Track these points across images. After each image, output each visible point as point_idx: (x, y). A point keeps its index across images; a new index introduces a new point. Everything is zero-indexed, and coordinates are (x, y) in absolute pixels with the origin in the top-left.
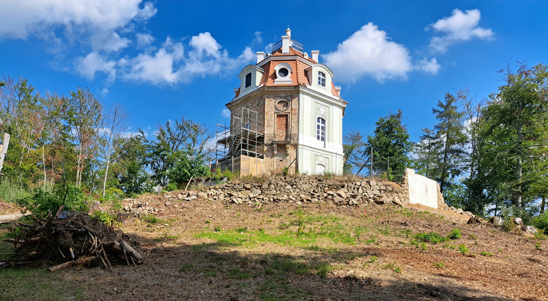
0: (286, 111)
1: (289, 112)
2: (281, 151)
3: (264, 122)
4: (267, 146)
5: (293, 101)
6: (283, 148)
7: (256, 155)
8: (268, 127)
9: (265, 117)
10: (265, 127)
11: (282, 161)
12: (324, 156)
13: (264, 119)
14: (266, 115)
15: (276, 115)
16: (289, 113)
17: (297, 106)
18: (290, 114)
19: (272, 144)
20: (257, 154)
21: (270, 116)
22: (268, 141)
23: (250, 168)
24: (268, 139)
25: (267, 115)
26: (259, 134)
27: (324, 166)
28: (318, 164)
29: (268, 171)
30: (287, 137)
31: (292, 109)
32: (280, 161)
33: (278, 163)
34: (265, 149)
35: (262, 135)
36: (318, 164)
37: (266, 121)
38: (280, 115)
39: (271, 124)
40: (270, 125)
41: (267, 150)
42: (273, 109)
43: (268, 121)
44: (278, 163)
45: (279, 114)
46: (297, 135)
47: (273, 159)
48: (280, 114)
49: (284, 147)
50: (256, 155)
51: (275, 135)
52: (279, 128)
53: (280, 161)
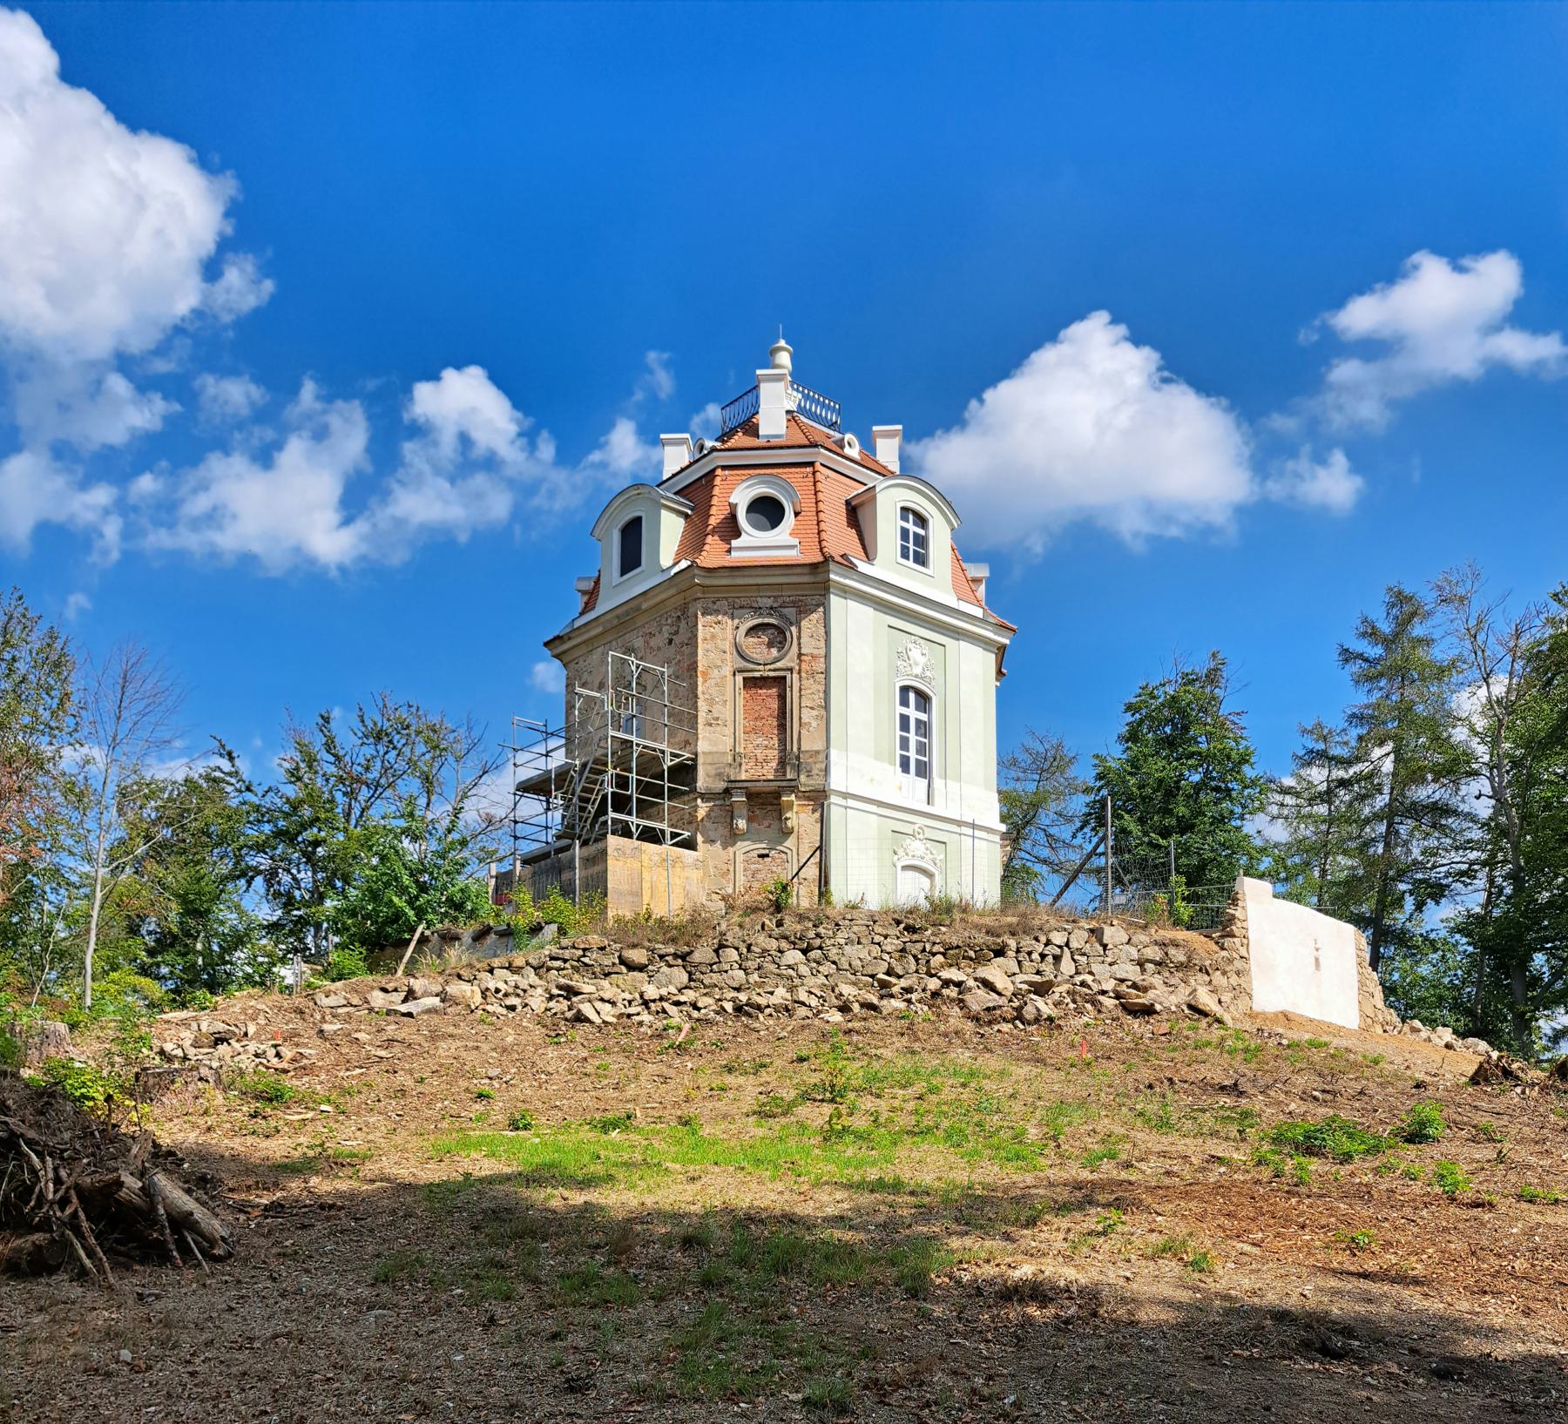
4: (708, 800)
6: (770, 808)
7: (668, 836)
8: (711, 725)
9: (700, 689)
10: (700, 727)
11: (767, 856)
12: (929, 834)
13: (696, 696)
19: (727, 791)
20: (668, 830)
25: (705, 681)
27: (930, 875)
28: (905, 868)
35: (688, 759)
36: (905, 868)
37: (700, 703)
40: (717, 719)
41: (708, 815)
43: (711, 702)
49: (775, 802)
50: (668, 836)
51: (738, 759)
52: (754, 730)
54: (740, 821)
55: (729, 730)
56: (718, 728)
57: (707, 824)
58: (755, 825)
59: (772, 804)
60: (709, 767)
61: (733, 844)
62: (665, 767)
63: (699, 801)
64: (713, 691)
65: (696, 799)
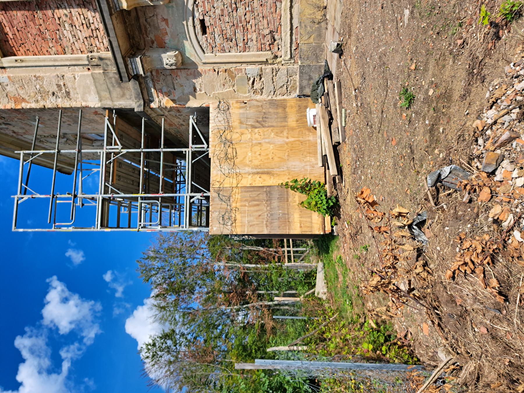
2: (157, 28)
3: (56, 109)
4: (150, 95)
6: (142, 20)
8: (68, 93)
9: (34, 105)
10: (74, 104)
11: (202, 22)
13: (43, 110)
19: (137, 77)
20: (192, 148)
21: (22, 87)
23: (259, 181)
24: (118, 90)
25: (24, 100)
26: (109, 133)
29: (256, 86)
32: (204, 32)
33: (218, 41)
34: (166, 102)
35: (110, 120)
37: (49, 105)
39: (54, 82)
40: (59, 86)
41: (168, 94)
43: (43, 93)
44: (218, 41)
49: (133, 14)
51: (95, 61)
52: (58, 41)
53: (204, 32)
54: (165, 61)
55: (68, 73)
56: (69, 85)
57: (177, 94)
58: (167, 39)
59: (138, 18)
60: (114, 94)
61: (194, 65)
62: (124, 151)
63: (153, 105)
64: (32, 91)
65: (152, 109)
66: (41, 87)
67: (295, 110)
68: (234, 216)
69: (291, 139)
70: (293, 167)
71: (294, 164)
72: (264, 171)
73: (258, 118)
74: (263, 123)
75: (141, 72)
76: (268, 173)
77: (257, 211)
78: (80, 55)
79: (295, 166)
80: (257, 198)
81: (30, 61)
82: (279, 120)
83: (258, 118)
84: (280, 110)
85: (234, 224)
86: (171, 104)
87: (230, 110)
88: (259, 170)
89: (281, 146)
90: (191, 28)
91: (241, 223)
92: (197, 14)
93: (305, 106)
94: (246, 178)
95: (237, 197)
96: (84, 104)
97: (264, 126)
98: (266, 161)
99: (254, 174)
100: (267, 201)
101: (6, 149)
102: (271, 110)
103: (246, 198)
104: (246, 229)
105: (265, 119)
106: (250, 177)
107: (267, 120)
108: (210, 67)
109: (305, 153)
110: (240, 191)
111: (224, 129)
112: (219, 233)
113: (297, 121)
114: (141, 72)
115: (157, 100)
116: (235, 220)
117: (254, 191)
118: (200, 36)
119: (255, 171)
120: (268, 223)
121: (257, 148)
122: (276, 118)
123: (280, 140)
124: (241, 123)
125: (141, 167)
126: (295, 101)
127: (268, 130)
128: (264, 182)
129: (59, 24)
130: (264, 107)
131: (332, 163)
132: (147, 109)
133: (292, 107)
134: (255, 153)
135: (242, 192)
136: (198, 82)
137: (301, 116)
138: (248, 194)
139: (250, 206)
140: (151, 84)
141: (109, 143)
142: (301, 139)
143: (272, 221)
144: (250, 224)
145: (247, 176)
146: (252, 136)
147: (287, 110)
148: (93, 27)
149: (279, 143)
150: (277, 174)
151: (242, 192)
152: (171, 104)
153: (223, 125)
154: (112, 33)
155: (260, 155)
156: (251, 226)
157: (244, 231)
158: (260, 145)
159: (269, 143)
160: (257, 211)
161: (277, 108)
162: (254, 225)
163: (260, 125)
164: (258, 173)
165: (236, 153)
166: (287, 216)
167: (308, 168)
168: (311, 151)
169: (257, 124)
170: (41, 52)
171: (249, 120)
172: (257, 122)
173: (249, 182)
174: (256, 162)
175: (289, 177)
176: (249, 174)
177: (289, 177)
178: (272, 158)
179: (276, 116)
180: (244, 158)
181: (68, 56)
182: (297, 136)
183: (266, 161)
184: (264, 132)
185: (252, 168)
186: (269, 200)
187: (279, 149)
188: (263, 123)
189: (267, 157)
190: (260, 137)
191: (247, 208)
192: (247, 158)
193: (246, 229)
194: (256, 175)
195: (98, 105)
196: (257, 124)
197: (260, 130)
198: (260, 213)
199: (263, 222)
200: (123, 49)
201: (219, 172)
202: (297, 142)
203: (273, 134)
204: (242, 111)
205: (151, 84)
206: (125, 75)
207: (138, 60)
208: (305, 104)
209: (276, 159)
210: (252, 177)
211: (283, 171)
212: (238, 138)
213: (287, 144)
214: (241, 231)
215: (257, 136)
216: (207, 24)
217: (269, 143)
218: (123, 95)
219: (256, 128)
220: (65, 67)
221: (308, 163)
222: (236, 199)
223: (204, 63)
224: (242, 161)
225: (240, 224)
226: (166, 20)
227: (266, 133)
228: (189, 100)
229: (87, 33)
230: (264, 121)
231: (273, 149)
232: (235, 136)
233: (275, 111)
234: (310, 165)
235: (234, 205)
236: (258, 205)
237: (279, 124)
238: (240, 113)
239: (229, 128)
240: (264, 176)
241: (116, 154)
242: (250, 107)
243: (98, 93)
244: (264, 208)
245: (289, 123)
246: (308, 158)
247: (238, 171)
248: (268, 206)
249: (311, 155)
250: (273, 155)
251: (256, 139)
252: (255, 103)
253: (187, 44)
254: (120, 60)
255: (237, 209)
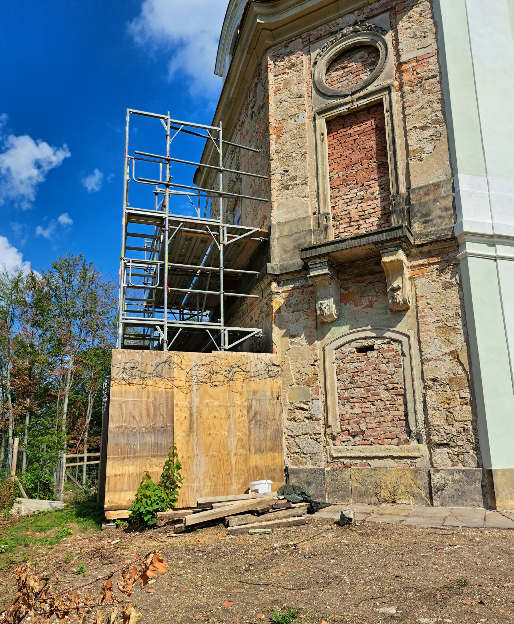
0: (371, 88)
1: (389, 82)
2: (362, 295)
5: (399, 27)
8: (287, 188)
9: (273, 148)
10: (274, 193)
11: (371, 348)
13: (268, 158)
14: (273, 138)
15: (321, 122)
16: (388, 88)
17: (431, 38)
18: (395, 95)
19: (306, 268)
20: (225, 330)
21: (293, 138)
22: (288, 256)
23: (180, 415)
24: (291, 246)
25: (279, 137)
26: (241, 232)
29: (298, 412)
30: (386, 215)
31: (400, 65)
33: (351, 367)
34: (278, 302)
35: (257, 234)
37: (274, 165)
38: (340, 117)
39: (300, 174)
40: (295, 178)
41: (287, 304)
42: (306, 100)
44: (351, 367)
45: (335, 112)
46: (445, 190)
47: (318, 344)
48: (343, 109)
52: (345, 182)
54: (325, 302)
55: (310, 189)
56: (296, 190)
57: (287, 314)
58: (350, 306)
59: (372, 273)
60: (286, 241)
61: (321, 337)
62: (221, 248)
63: (274, 285)
64: (289, 147)
65: (270, 284)
66: (294, 159)
67: (270, 465)
68: (135, 382)
69: (233, 459)
70: (198, 463)
71: (202, 464)
72: (193, 424)
73: (260, 414)
74: (254, 421)
75: (312, 274)
76: (191, 428)
77: (140, 414)
78: (330, 205)
79: (200, 465)
80: (158, 413)
81: (322, 149)
82: (257, 442)
83: (260, 414)
84: (269, 444)
85: (124, 382)
86: (276, 306)
87: (269, 379)
88: (195, 417)
89: (225, 446)
90: (363, 334)
91: (126, 392)
92: (379, 342)
93: (274, 477)
94: (186, 399)
95: (161, 386)
96: (275, 205)
97: (250, 422)
98: (206, 425)
99: (191, 409)
100: (153, 428)
101: (224, 111)
102: (269, 431)
103: (158, 398)
104: (116, 399)
105: (258, 424)
106: (187, 404)
107: (258, 426)
108: (320, 356)
109: (215, 479)
110: (168, 390)
111: (247, 370)
112: (113, 362)
113: (256, 467)
114: (312, 274)
115: (280, 290)
116: (129, 384)
117: (168, 410)
118: (355, 345)
119: (195, 410)
120: (123, 429)
121: (223, 413)
122: (260, 438)
123: (232, 444)
124: (254, 392)
125: (201, 267)
126: (280, 464)
127: (245, 428)
128: (179, 424)
129: (363, 185)
130: (273, 423)
131: (202, 517)
132: (270, 278)
133: (273, 460)
134: (217, 411)
135: (167, 393)
136: (302, 340)
137: (262, 473)
138: (163, 401)
139: (147, 405)
140: (298, 284)
141: (230, 231)
142: (234, 473)
143: (126, 435)
144: (123, 405)
145: (188, 400)
146: (238, 406)
147: (270, 453)
148: (361, 222)
149: (229, 443)
150: (189, 441)
151: (167, 393)
152: (276, 306)
153: (251, 369)
154: (355, 243)
155: (215, 417)
156: (121, 405)
157: (114, 396)
158: (227, 416)
159: (230, 429)
160: (140, 414)
161: (272, 439)
162: (122, 410)
163: (251, 417)
164: (191, 415)
165: (218, 386)
166: (132, 455)
167: (196, 484)
168: (218, 487)
169: (252, 414)
170: (332, 161)
171: (258, 402)
172: (256, 414)
173: (180, 404)
174: (205, 412)
175: (185, 458)
176: (190, 403)
177: (185, 458)
178: (210, 434)
179: (262, 438)
180: (211, 396)
181: (329, 192)
182: (238, 467)
183: (206, 425)
184: (243, 422)
185: (198, 407)
186: (154, 431)
187: (222, 443)
188: (254, 421)
189: (212, 426)
190: (237, 417)
191: (145, 399)
192: (211, 400)
193: (116, 399)
194: (188, 413)
195: (274, 221)
196: (253, 413)
197: (245, 418)
198: (137, 418)
199: (125, 422)
200: (338, 254)
201: (193, 364)
202: (230, 468)
203: (241, 434)
204: (268, 393)
205: (298, 284)
206: (308, 254)
207: (326, 271)
208: (276, 477)
209: (210, 439)
210: (187, 407)
211: (193, 450)
212: (236, 389)
213: (228, 454)
214: (114, 392)
215: (238, 413)
216: (369, 354)
217: (230, 429)
218: (285, 251)
219: (248, 412)
220: (316, 187)
221: (202, 484)
222: (157, 385)
223: (324, 348)
224: (208, 393)
225: (123, 391)
226: (371, 305)
227: (242, 425)
228: (281, 328)
229: (355, 215)
230: (256, 422)
231: (222, 434)
232: (238, 384)
233: (269, 438)
234: (200, 487)
235: (150, 382)
236: (148, 415)
237: (252, 443)
238: (265, 392)
239: (248, 378)
240: (187, 423)
241: (218, 237)
242: (273, 404)
243: (287, 222)
244: (145, 423)
245: (253, 456)
246: (210, 484)
247: (195, 388)
248: (146, 428)
249: (213, 487)
250: (214, 435)
251: (234, 412)
252: (278, 411)
253: (345, 329)
254: (325, 250)
255: (144, 386)
